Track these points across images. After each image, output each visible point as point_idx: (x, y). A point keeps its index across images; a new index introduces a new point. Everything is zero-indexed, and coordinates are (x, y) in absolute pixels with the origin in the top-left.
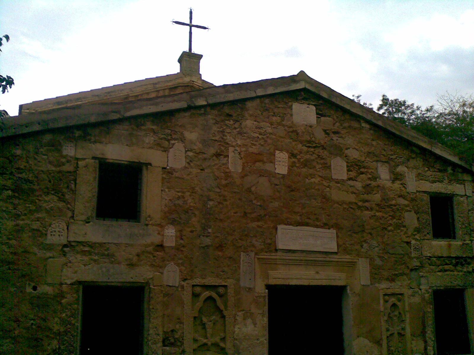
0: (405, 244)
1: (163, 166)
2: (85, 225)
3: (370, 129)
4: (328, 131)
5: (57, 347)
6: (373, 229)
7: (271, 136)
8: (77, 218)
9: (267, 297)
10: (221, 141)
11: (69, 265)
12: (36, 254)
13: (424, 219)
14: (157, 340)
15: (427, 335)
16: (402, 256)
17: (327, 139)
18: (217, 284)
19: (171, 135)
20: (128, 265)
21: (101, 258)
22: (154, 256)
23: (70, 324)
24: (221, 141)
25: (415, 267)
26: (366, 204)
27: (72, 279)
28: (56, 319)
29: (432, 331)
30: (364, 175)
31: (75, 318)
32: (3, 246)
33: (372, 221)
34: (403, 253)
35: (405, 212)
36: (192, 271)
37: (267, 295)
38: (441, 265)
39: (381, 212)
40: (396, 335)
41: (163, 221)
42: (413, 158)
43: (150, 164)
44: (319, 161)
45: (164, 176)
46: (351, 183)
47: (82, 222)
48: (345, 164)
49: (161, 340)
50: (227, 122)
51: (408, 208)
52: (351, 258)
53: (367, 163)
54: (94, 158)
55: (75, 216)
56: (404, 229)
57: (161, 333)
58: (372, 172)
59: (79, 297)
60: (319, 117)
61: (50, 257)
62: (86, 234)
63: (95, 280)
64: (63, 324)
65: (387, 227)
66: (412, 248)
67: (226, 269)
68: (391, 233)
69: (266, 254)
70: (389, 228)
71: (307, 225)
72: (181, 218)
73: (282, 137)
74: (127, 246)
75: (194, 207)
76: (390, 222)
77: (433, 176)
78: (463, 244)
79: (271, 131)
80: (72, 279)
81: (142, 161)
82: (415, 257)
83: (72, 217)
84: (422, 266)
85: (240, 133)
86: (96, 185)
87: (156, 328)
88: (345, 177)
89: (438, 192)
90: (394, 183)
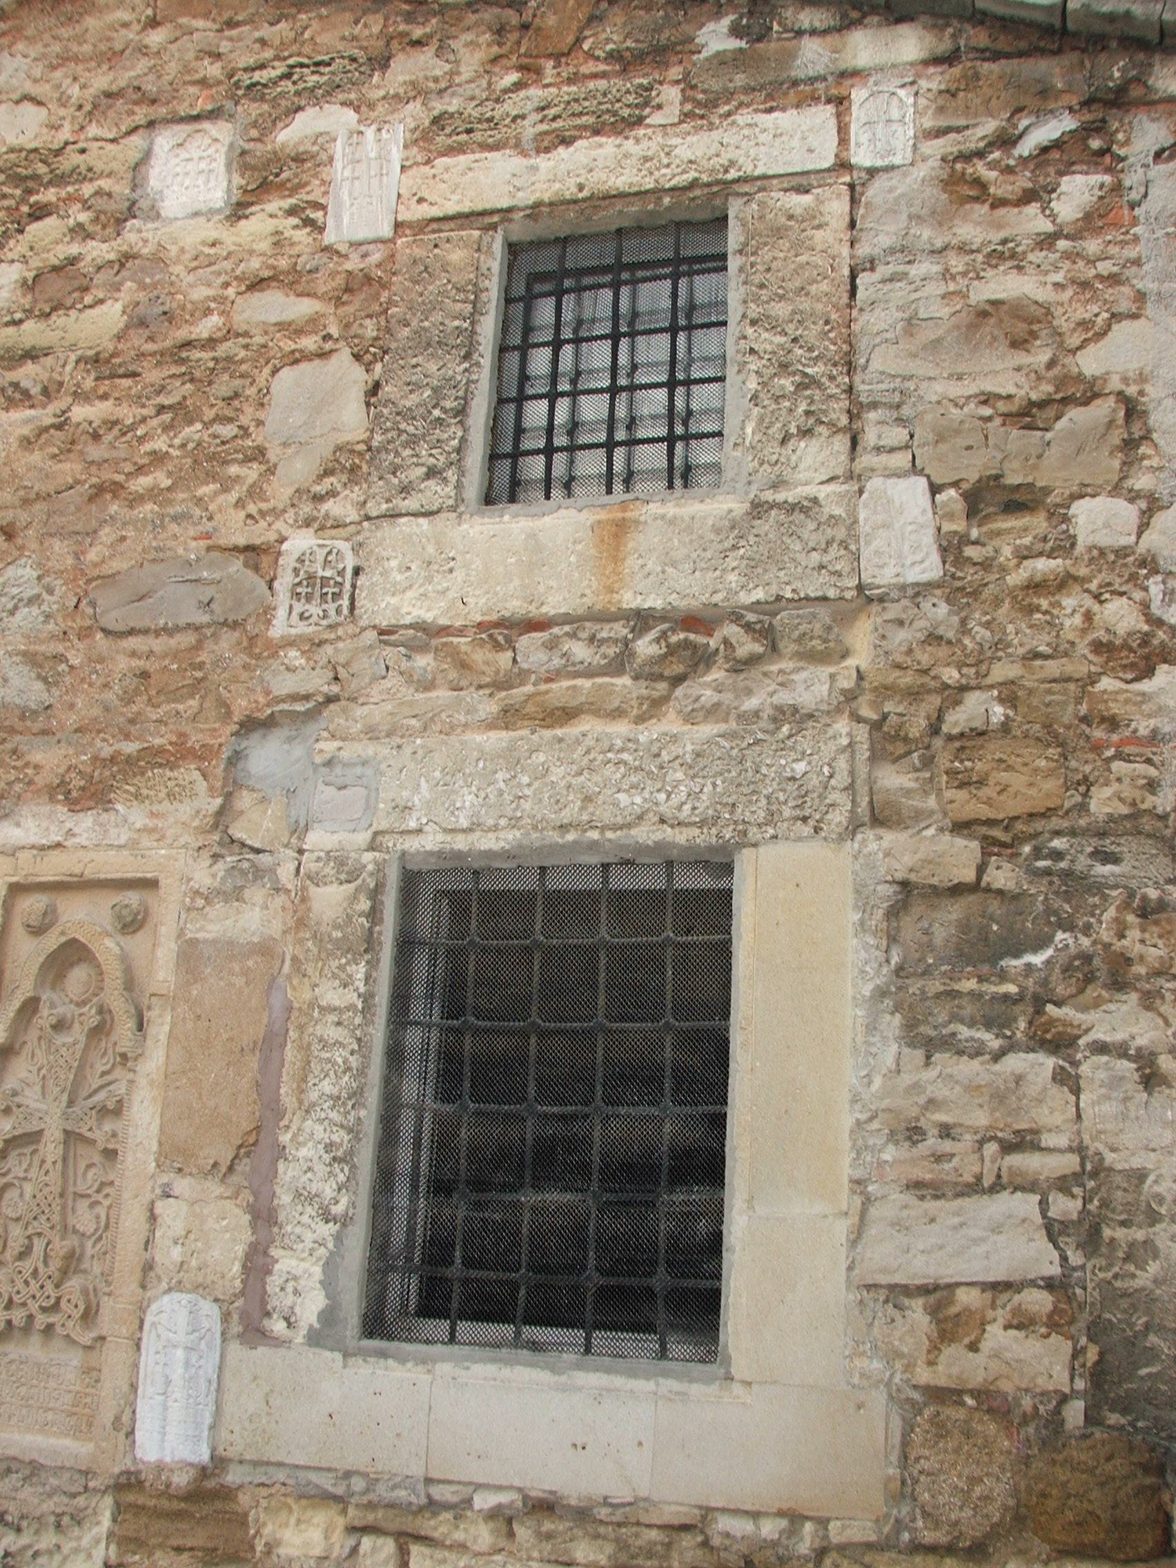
0: (236, 565)
6: (26, 502)
13: (415, 387)
15: (287, 1173)
16: (189, 639)
25: (285, 706)
29: (329, 1147)
30: (51, 221)
33: (36, 457)
35: (275, 372)
39: (105, 397)
40: (51, 1149)
42: (418, 43)
51: (309, 343)
53: (83, 151)
56: (251, 473)
58: (98, 193)
65: (129, 475)
66: (284, 582)
70: (142, 483)
76: (160, 444)
77: (552, 112)
78: (758, 509)
82: (290, 643)
89: (585, 193)
90: (240, 218)
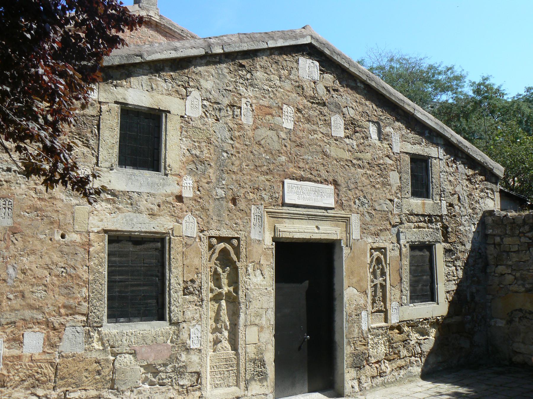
1: (181, 115)
2: (110, 173)
3: (364, 89)
4: (329, 89)
5: (87, 295)
7: (279, 89)
8: (101, 165)
9: (274, 249)
10: (234, 92)
11: (95, 212)
12: (63, 201)
14: (177, 289)
17: (328, 96)
18: (230, 236)
19: (188, 83)
20: (149, 215)
21: (125, 207)
22: (173, 207)
23: (99, 272)
24: (234, 92)
26: (360, 162)
27: (99, 227)
28: (85, 267)
31: (102, 266)
32: (31, 191)
34: (387, 210)
36: (208, 222)
37: (274, 247)
38: (416, 222)
41: (182, 171)
43: (169, 112)
44: (321, 118)
45: (182, 125)
46: (347, 140)
47: (106, 169)
48: (342, 122)
49: (182, 289)
50: (240, 72)
52: (345, 213)
54: (116, 102)
55: (99, 162)
57: (181, 282)
58: (365, 131)
59: (105, 245)
60: (322, 74)
61: (77, 205)
62: (110, 182)
63: (119, 229)
64: (91, 272)
66: (395, 205)
67: (237, 221)
68: (378, 191)
69: (273, 208)
71: (310, 180)
72: (197, 169)
73: (289, 91)
74: (149, 195)
75: (209, 158)
79: (279, 85)
80: (99, 227)
81: (161, 108)
83: (97, 164)
84: (401, 223)
85: (251, 85)
86: (117, 130)
87: (177, 277)
88: (342, 135)
